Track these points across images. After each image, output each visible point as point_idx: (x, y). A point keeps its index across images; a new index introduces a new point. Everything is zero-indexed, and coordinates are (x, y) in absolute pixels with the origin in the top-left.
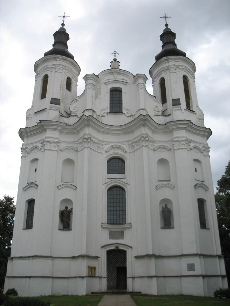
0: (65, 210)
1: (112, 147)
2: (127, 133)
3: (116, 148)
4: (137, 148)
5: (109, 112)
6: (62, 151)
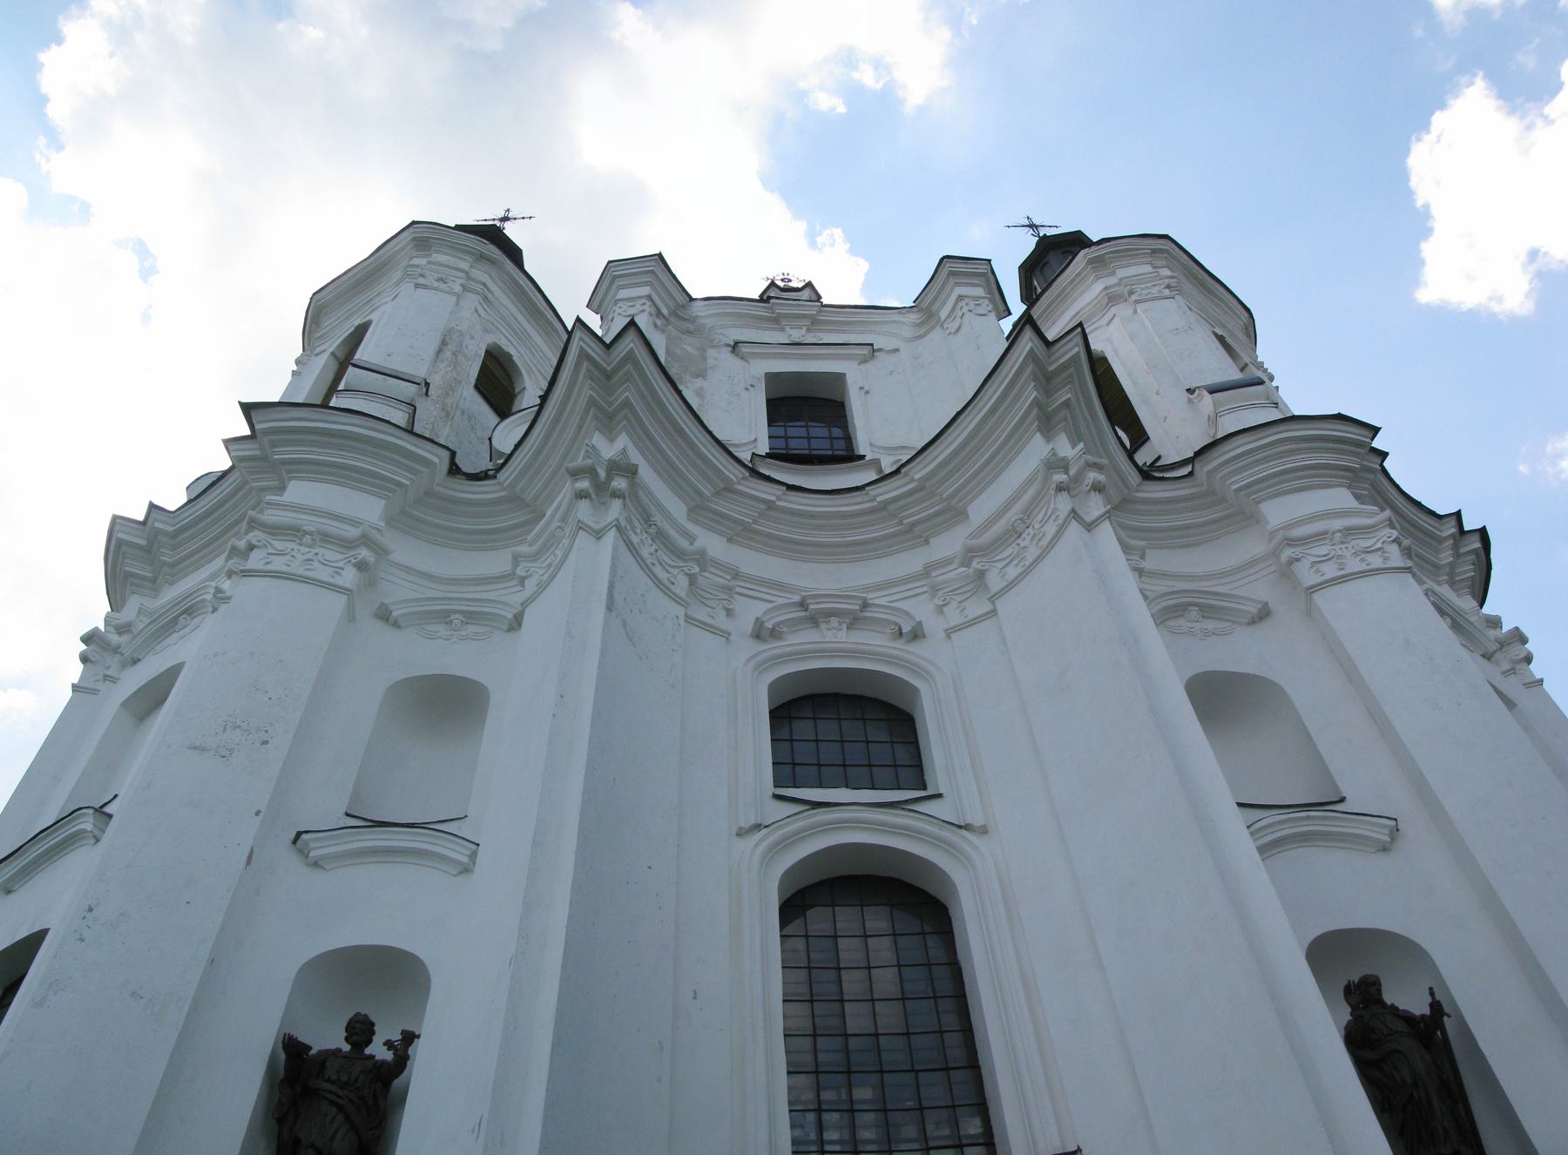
0: (336, 1053)
1: (803, 614)
2: (916, 535)
3: (834, 621)
4: (1012, 572)
5: (768, 456)
6: (396, 625)
